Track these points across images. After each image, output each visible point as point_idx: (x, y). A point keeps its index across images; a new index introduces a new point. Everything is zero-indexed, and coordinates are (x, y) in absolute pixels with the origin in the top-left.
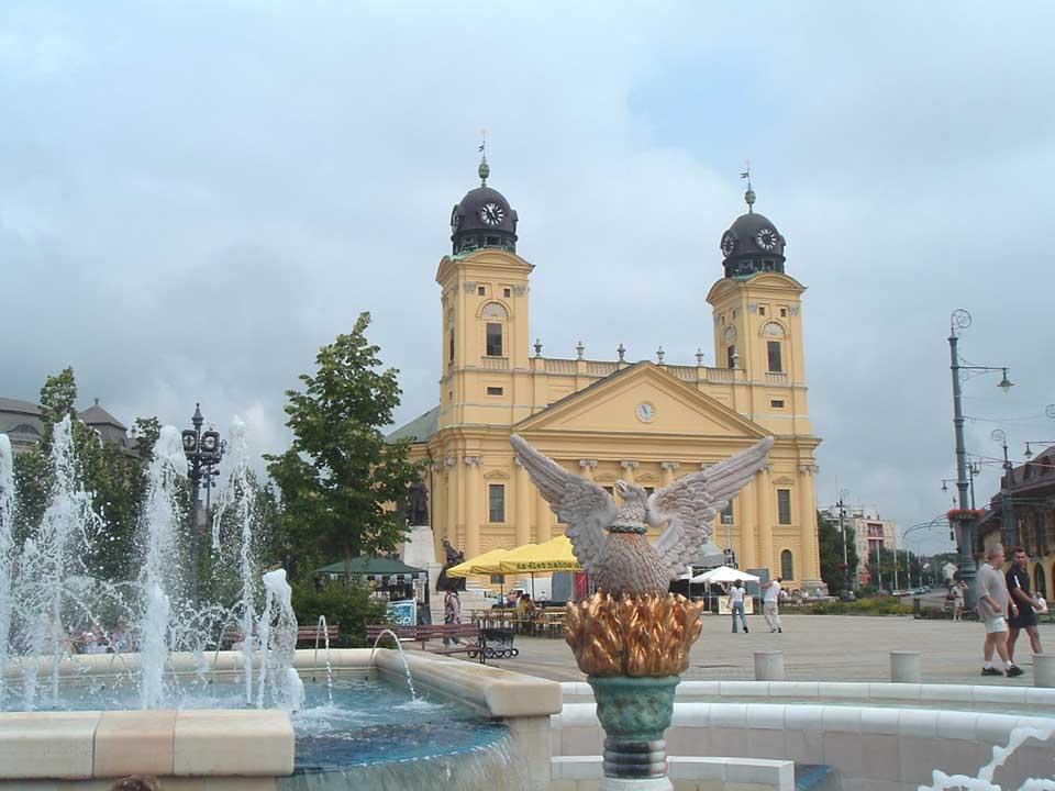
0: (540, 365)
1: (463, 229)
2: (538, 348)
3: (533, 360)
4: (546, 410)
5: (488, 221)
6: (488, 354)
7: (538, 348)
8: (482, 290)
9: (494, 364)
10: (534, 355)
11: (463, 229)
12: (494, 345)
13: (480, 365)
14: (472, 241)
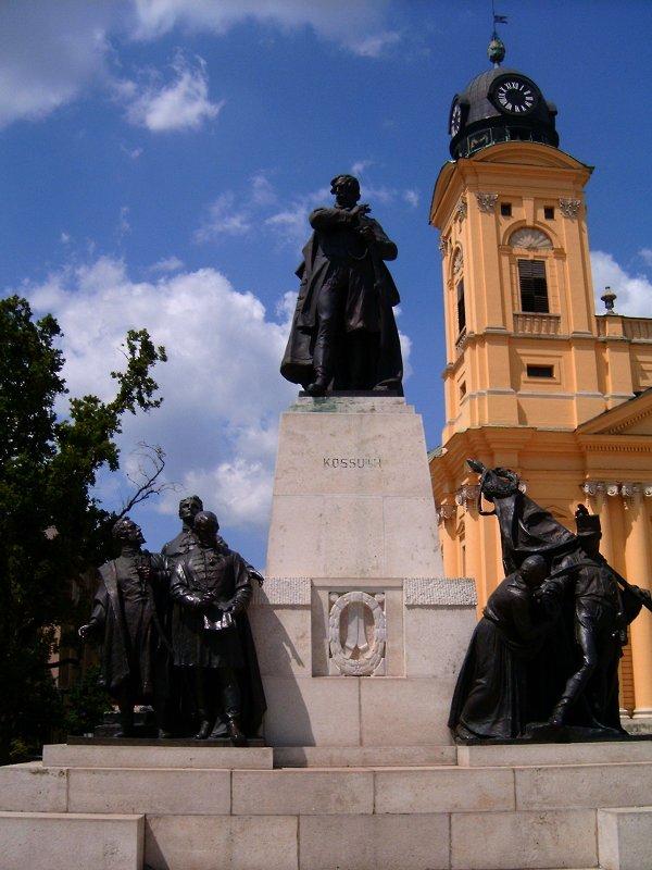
0: (614, 330)
1: (470, 121)
2: (609, 300)
3: (601, 320)
4: (632, 399)
5: (509, 107)
6: (523, 310)
7: (609, 300)
8: (506, 210)
9: (532, 328)
10: (600, 309)
11: (470, 121)
12: (534, 294)
13: (510, 329)
14: (485, 138)
